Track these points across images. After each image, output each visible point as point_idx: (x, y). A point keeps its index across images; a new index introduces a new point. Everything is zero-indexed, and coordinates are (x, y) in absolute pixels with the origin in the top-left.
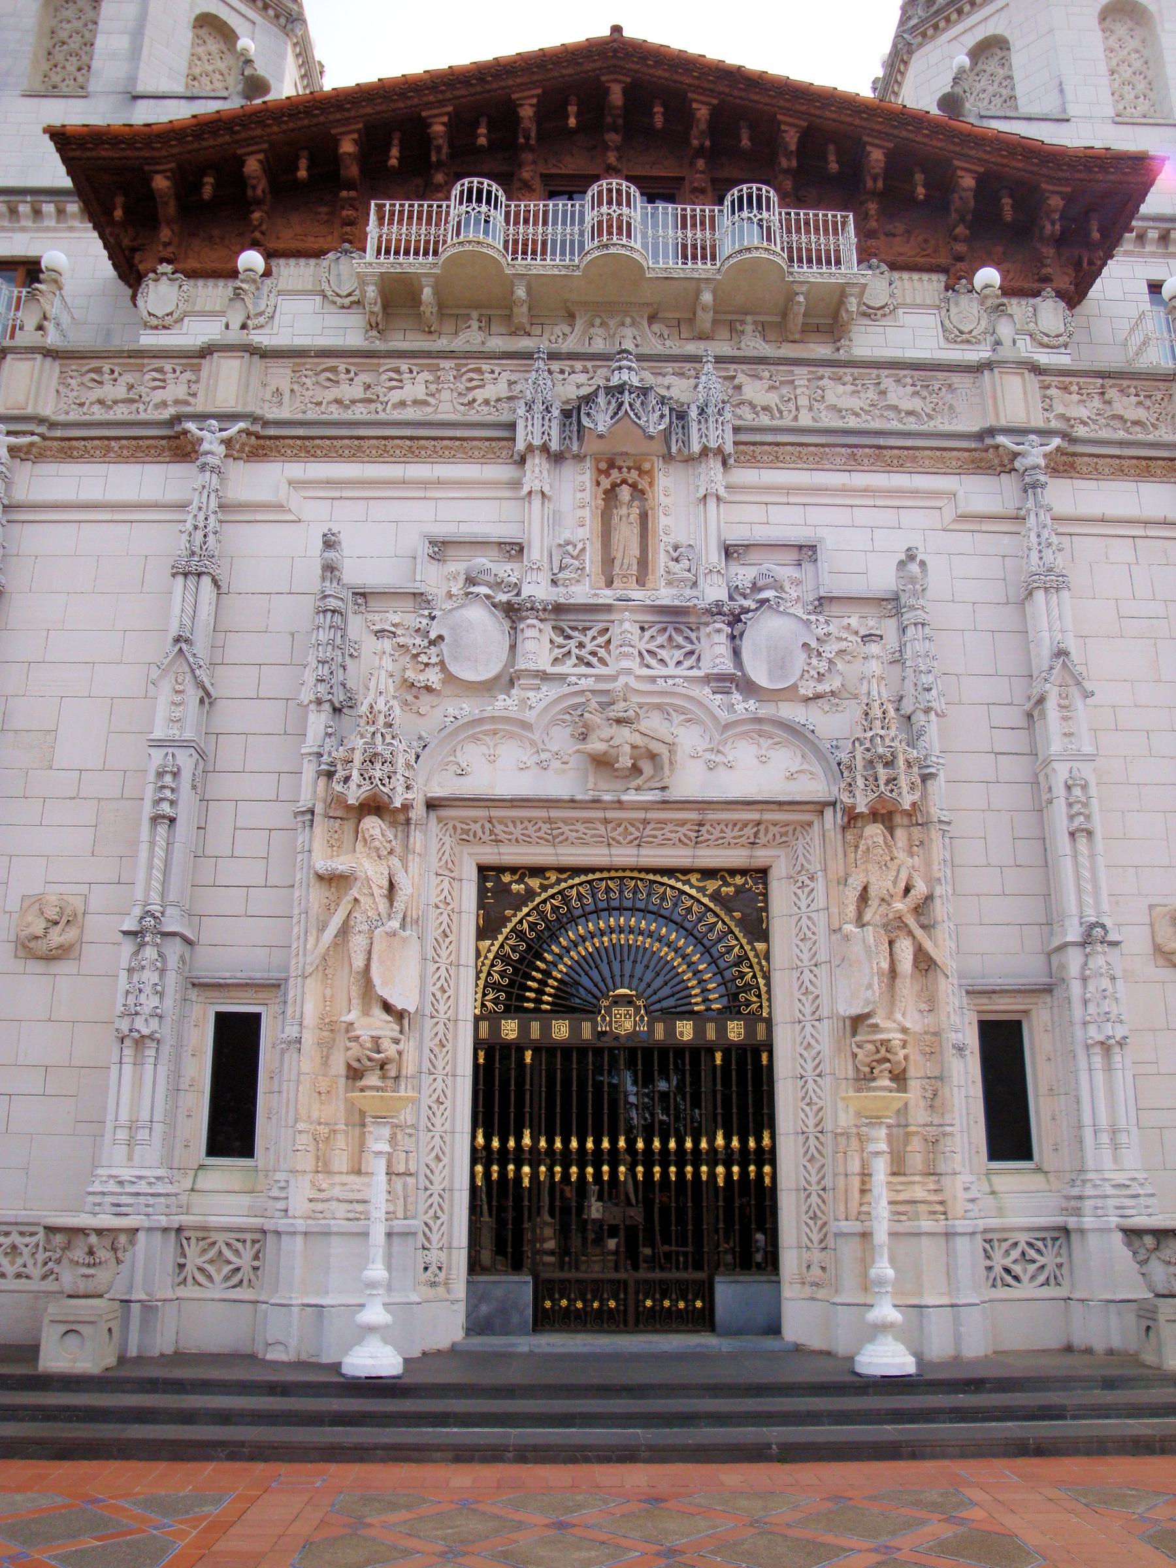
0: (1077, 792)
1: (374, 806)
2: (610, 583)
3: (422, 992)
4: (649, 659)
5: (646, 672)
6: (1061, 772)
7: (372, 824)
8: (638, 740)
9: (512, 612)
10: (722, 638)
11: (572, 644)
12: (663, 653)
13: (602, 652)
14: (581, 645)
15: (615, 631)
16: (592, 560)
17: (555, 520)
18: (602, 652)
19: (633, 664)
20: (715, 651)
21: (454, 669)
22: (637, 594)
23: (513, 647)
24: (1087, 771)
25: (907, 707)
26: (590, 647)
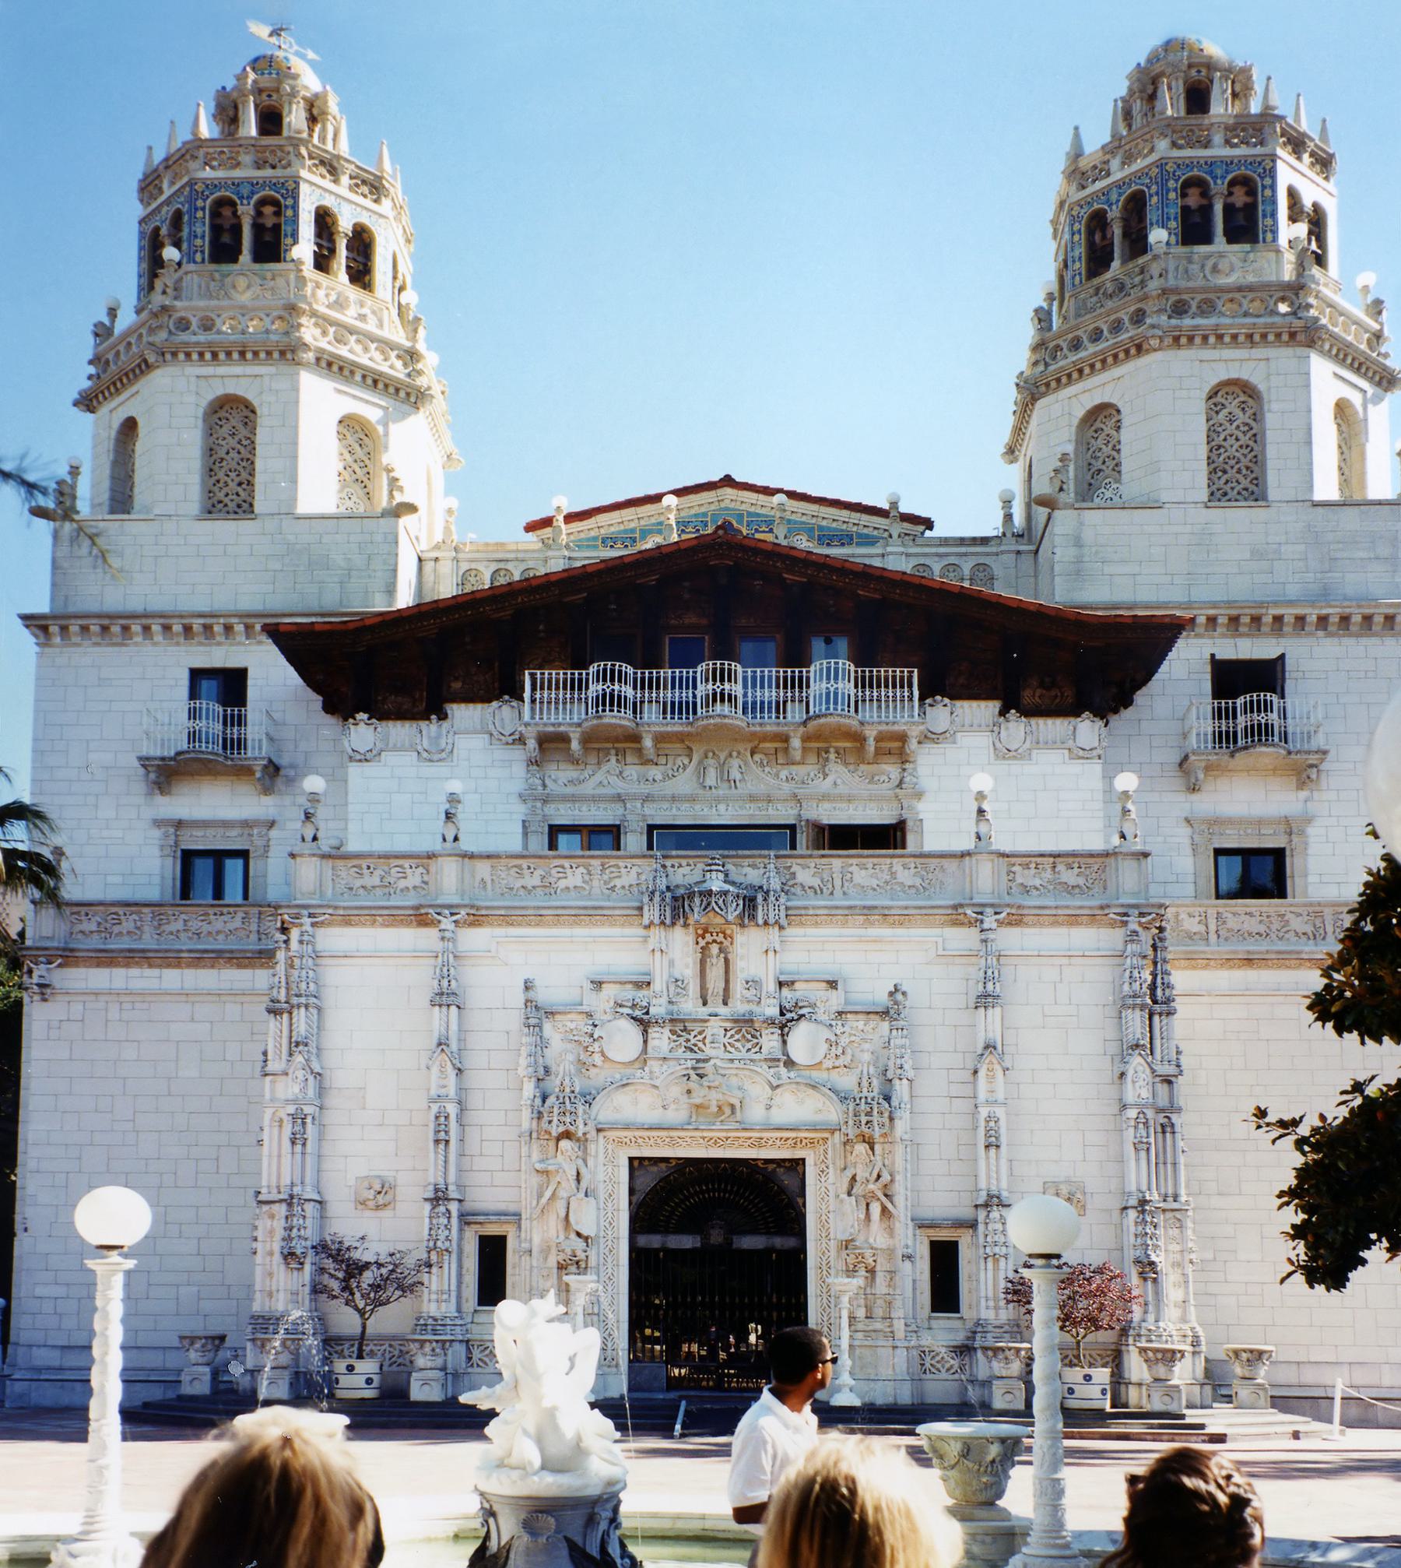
0: (992, 1124)
1: (567, 1135)
2: (705, 1004)
3: (598, 1225)
4: (729, 1048)
5: (730, 1056)
6: (984, 1112)
7: (564, 1144)
8: (720, 1096)
9: (644, 1024)
10: (776, 1037)
11: (682, 1039)
12: (738, 1045)
13: (700, 1044)
14: (688, 1040)
15: (708, 1033)
16: (693, 988)
17: (671, 963)
18: (700, 1044)
19: (720, 1052)
20: (770, 1041)
21: (610, 1055)
22: (723, 1010)
23: (645, 1042)
24: (1000, 1112)
25: (890, 1075)
26: (693, 1041)
